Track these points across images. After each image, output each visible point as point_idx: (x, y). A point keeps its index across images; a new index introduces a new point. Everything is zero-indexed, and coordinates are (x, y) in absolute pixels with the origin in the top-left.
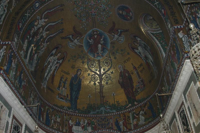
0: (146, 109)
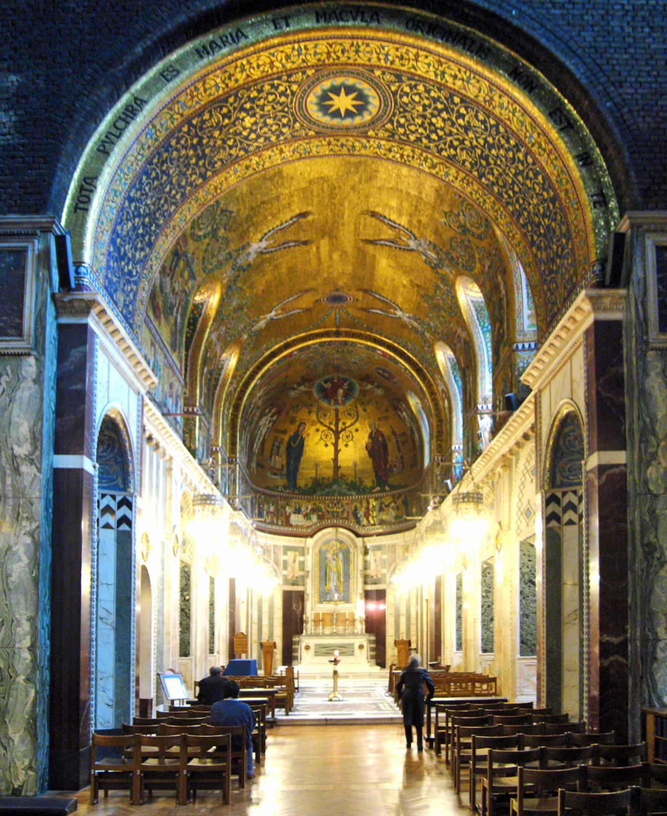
0: (399, 502)
